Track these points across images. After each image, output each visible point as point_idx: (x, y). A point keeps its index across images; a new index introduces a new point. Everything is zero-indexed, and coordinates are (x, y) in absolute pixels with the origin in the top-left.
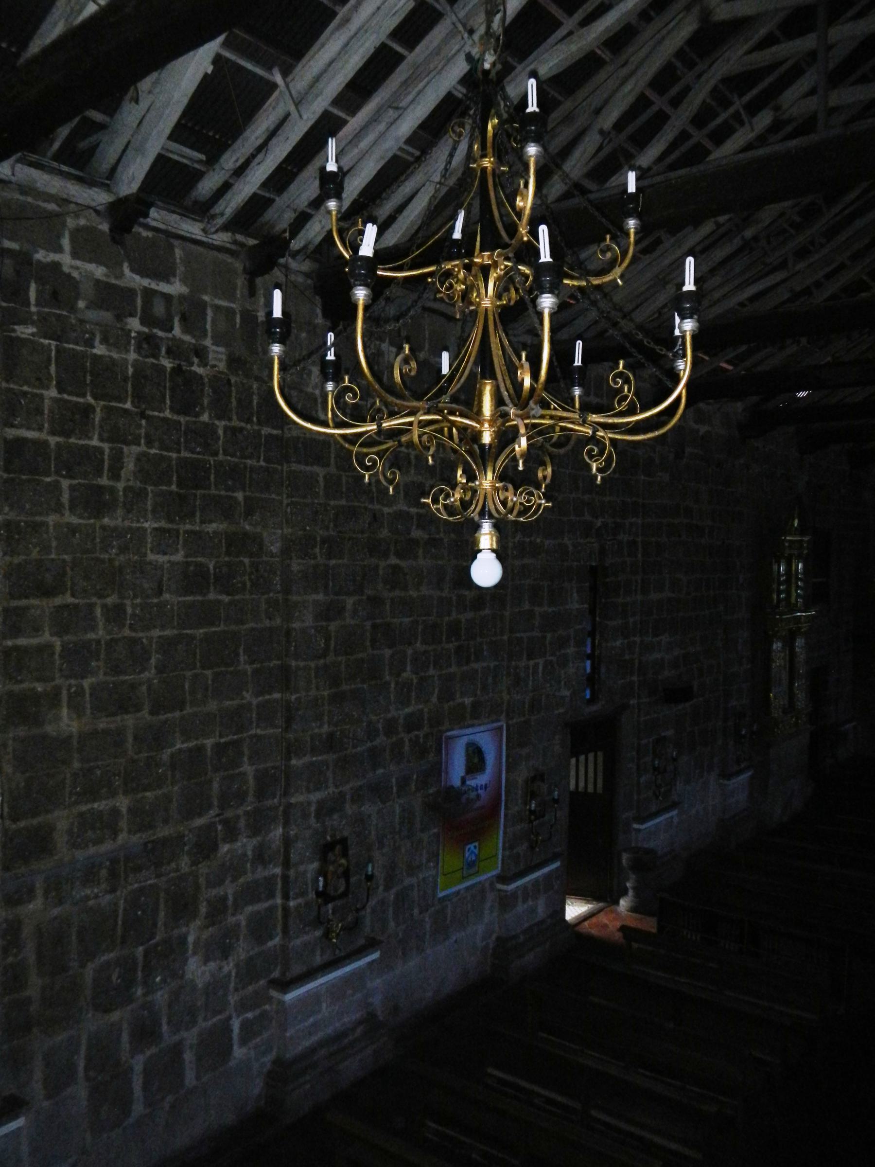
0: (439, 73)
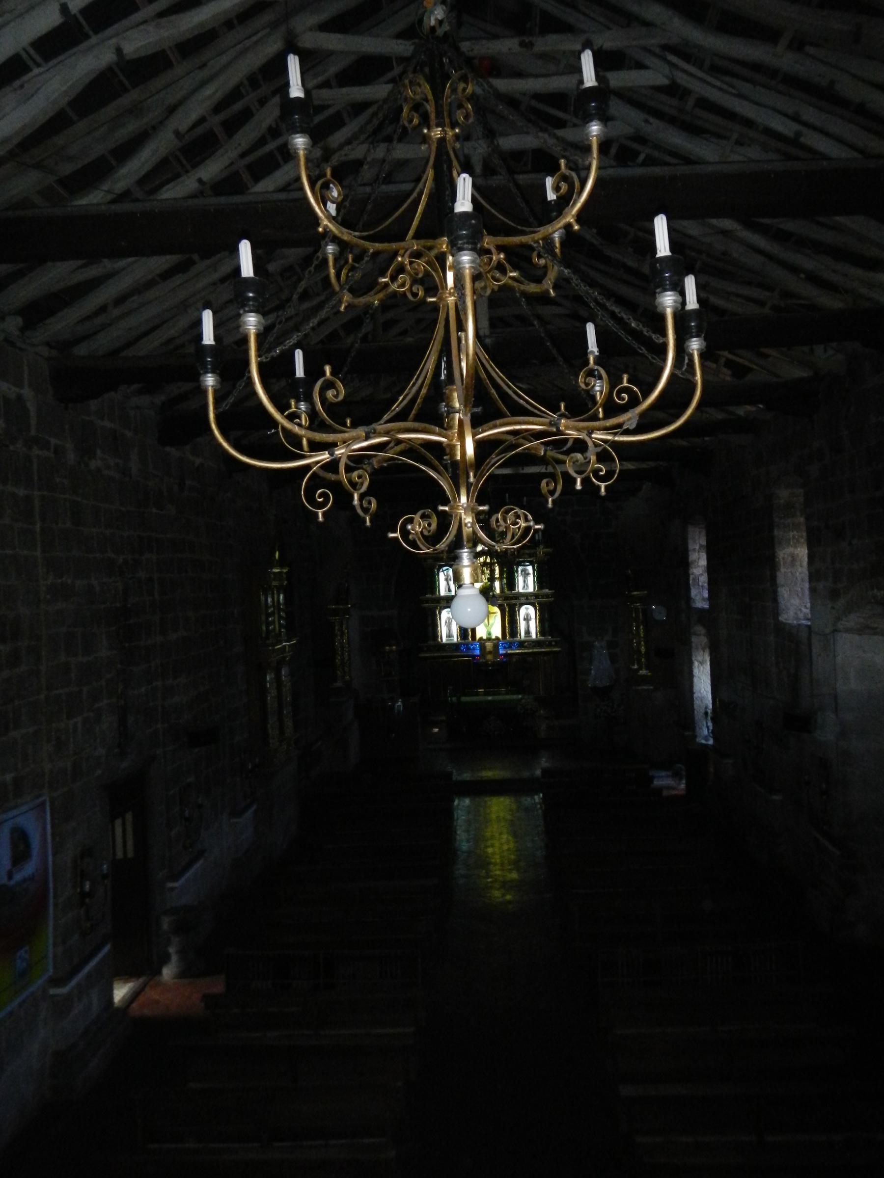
0: (20, 15)
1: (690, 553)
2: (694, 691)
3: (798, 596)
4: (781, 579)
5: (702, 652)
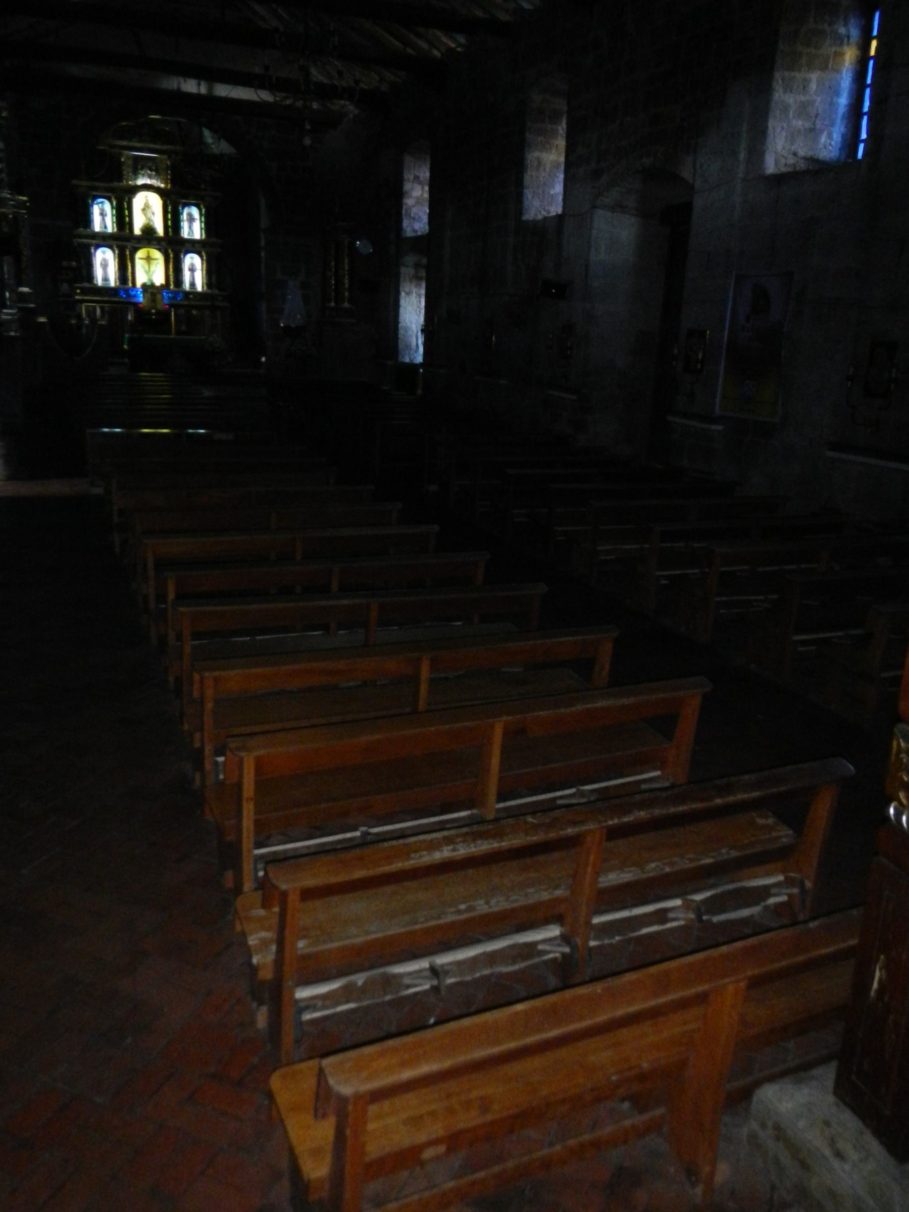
1: (405, 183)
2: (400, 320)
3: (539, 198)
4: (527, 180)
5: (409, 283)
